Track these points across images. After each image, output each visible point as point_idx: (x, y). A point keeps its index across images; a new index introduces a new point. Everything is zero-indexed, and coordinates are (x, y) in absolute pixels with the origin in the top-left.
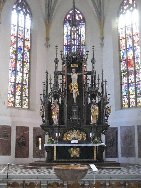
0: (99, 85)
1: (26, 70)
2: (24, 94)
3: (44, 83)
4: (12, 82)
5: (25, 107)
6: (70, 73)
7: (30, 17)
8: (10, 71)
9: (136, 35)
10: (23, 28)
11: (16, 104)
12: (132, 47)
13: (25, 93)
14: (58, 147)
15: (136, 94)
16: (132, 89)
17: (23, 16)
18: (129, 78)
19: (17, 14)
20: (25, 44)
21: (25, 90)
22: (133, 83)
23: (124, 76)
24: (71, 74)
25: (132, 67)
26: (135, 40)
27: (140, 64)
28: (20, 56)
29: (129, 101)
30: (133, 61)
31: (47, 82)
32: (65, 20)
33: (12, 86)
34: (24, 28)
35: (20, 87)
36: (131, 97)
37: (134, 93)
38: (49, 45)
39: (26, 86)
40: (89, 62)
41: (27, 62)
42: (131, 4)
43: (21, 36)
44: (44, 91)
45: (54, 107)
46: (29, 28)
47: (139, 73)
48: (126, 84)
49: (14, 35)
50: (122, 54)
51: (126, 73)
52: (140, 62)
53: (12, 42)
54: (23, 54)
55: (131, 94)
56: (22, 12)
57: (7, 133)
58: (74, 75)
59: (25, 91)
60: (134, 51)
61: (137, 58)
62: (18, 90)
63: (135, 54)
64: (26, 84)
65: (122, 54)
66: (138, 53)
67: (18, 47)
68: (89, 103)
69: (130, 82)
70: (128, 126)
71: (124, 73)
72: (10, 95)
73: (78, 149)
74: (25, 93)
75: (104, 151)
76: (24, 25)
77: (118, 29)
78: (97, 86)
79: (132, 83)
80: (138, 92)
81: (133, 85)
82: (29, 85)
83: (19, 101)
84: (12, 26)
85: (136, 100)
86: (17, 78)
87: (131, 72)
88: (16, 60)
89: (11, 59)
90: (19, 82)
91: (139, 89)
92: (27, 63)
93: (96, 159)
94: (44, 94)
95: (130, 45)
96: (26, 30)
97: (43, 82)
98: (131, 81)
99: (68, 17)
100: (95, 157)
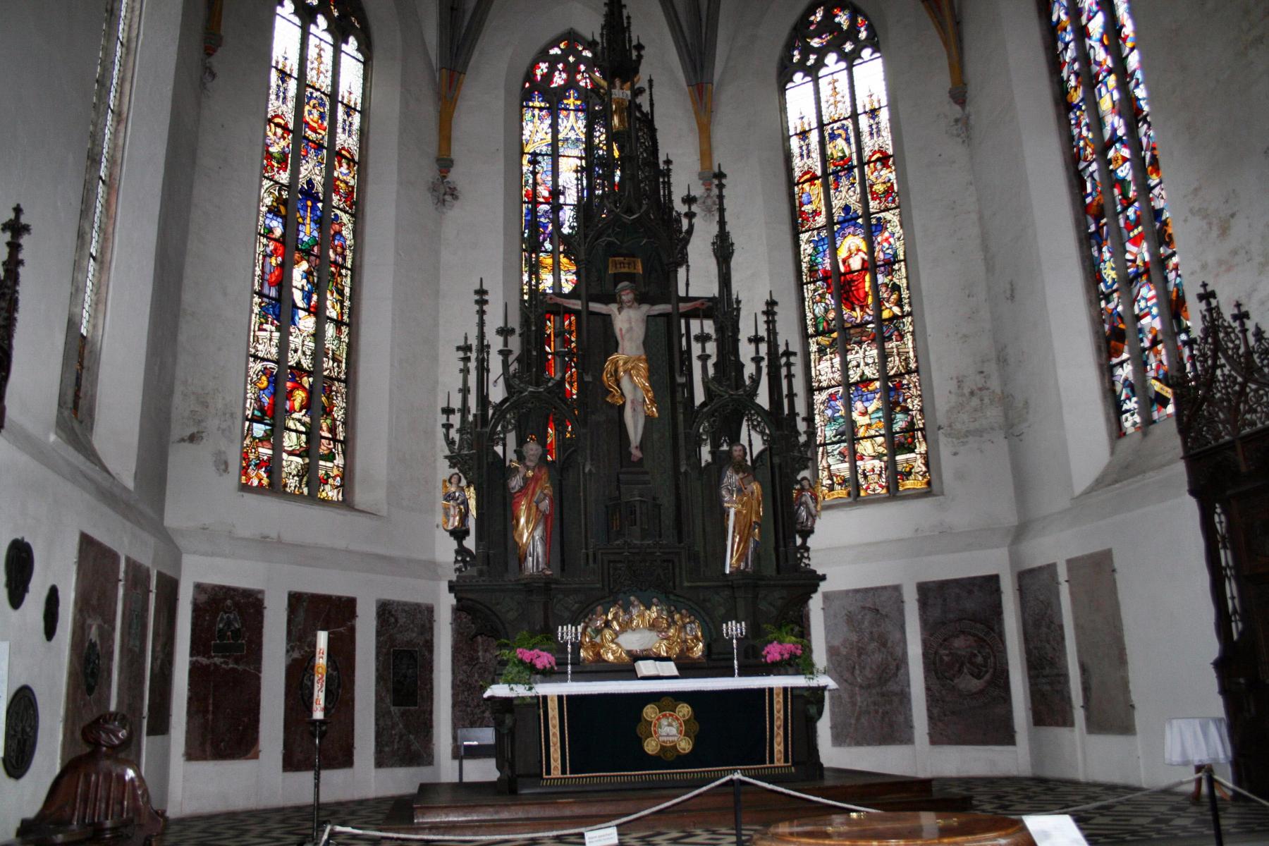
0: (759, 369)
1: (338, 307)
2: (325, 428)
3: (466, 348)
4: (263, 359)
5: (330, 493)
6: (606, 303)
7: (358, 50)
8: (257, 299)
9: (878, 160)
10: (323, 93)
11: (284, 475)
12: (859, 217)
13: (329, 421)
14: (569, 697)
15: (890, 435)
16: (867, 413)
17: (328, 38)
18: (849, 357)
19: (297, 20)
20: (336, 174)
21: (333, 405)
22: (872, 380)
23: (822, 351)
24: (613, 308)
25: (862, 309)
26: (871, 186)
27: (905, 294)
28: (308, 232)
29: (854, 468)
30: (867, 278)
31: (483, 348)
32: (527, 85)
33: (264, 378)
34: (333, 96)
35: (307, 386)
36: (865, 447)
37: (882, 432)
38: (453, 193)
39: (334, 388)
40: (700, 251)
41: (343, 267)
42: (845, 27)
43: (316, 132)
44: (465, 391)
45: (525, 479)
46: (356, 98)
47: (901, 337)
48: (832, 391)
49: (282, 122)
50: (810, 251)
51: (835, 335)
52: (903, 283)
53: (270, 156)
54: (322, 222)
55: (861, 433)
56: (322, 21)
57: (237, 634)
58: (625, 313)
59: (327, 412)
61: (890, 264)
62: (297, 405)
63: (878, 248)
64: (334, 374)
65: (806, 249)
66: (892, 239)
67: (302, 182)
68: (703, 464)
69: (854, 376)
70: (866, 591)
71: (820, 338)
72: (255, 425)
73: (685, 710)
74: (329, 421)
75: (820, 713)
76: (329, 81)
77: (786, 135)
78: (750, 369)
79: (865, 381)
80: (900, 422)
81: (874, 392)
82: (350, 380)
83: (299, 460)
84: (274, 75)
85: (891, 466)
86: (295, 341)
87: (858, 330)
88: (288, 246)
89: (264, 241)
90: (299, 363)
91: (906, 410)
92: (344, 272)
93: (786, 760)
94: (465, 410)
95: (846, 208)
96: (340, 109)
97: (462, 343)
98: (859, 371)
99: (539, 72)
100: (779, 747)
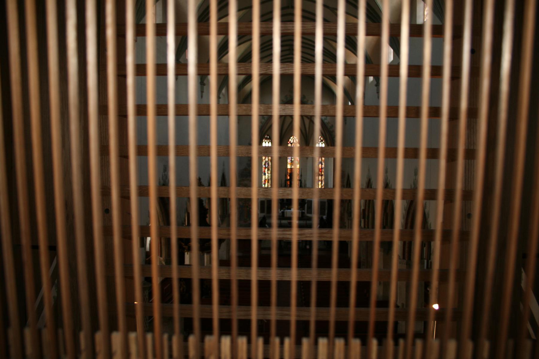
28: (267, 166)
60: (322, 164)
88: (265, 168)
